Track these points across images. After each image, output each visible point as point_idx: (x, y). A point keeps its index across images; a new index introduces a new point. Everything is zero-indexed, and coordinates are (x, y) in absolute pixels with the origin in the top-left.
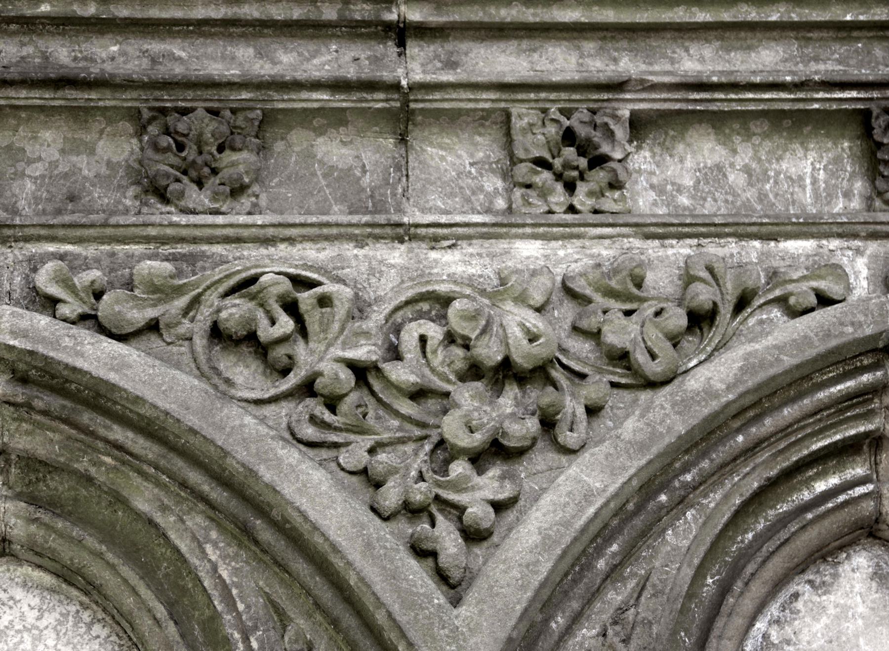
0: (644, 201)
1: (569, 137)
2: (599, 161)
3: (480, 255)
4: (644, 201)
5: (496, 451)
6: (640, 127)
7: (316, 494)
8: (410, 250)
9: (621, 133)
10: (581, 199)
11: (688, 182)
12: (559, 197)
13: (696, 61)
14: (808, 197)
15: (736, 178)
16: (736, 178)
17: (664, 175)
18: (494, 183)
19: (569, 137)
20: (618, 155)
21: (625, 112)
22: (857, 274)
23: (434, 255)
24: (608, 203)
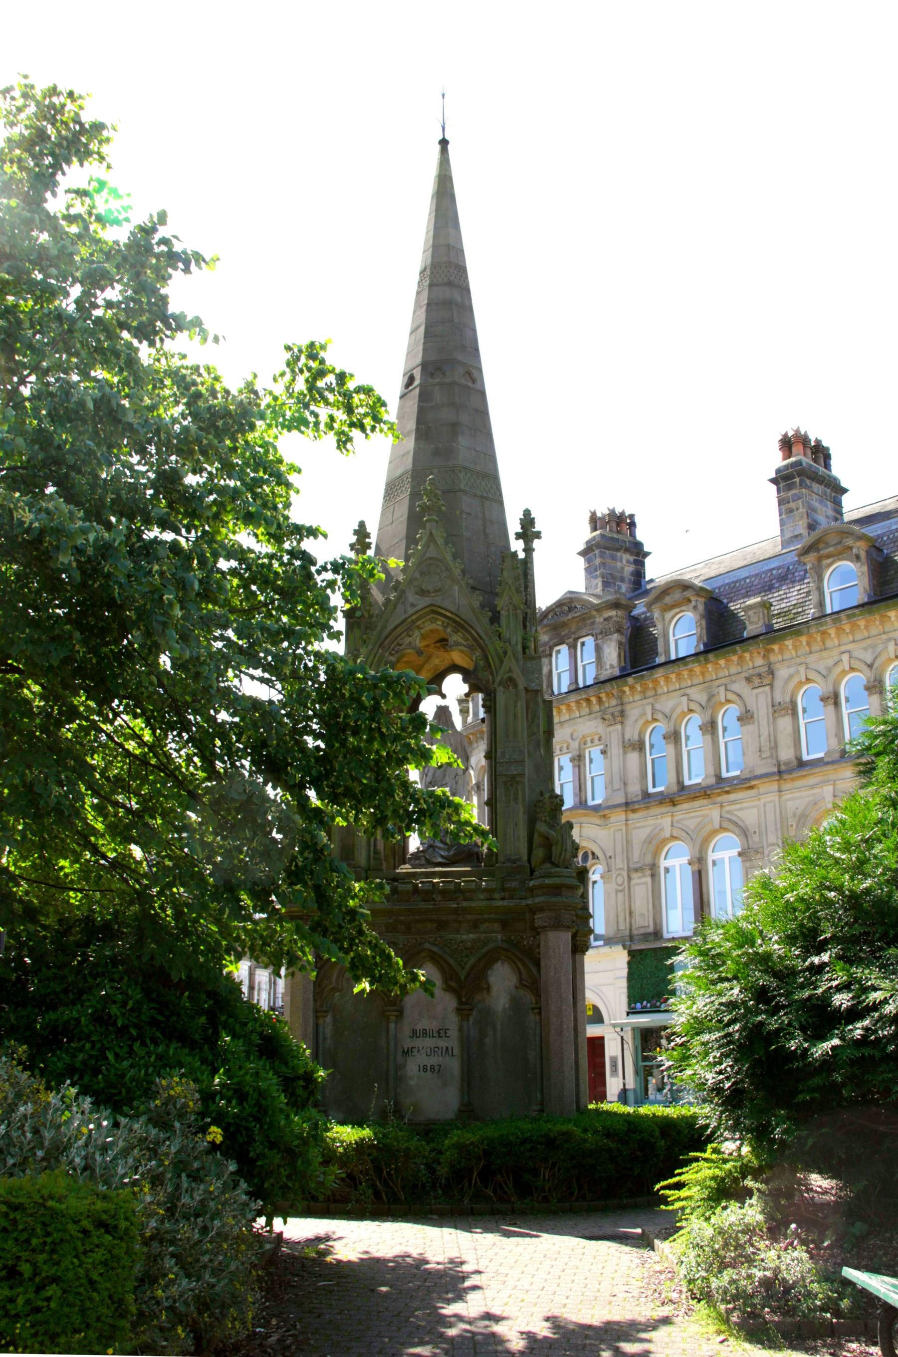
5: (467, 956)
7: (451, 961)
13: (486, 916)
17: (483, 927)
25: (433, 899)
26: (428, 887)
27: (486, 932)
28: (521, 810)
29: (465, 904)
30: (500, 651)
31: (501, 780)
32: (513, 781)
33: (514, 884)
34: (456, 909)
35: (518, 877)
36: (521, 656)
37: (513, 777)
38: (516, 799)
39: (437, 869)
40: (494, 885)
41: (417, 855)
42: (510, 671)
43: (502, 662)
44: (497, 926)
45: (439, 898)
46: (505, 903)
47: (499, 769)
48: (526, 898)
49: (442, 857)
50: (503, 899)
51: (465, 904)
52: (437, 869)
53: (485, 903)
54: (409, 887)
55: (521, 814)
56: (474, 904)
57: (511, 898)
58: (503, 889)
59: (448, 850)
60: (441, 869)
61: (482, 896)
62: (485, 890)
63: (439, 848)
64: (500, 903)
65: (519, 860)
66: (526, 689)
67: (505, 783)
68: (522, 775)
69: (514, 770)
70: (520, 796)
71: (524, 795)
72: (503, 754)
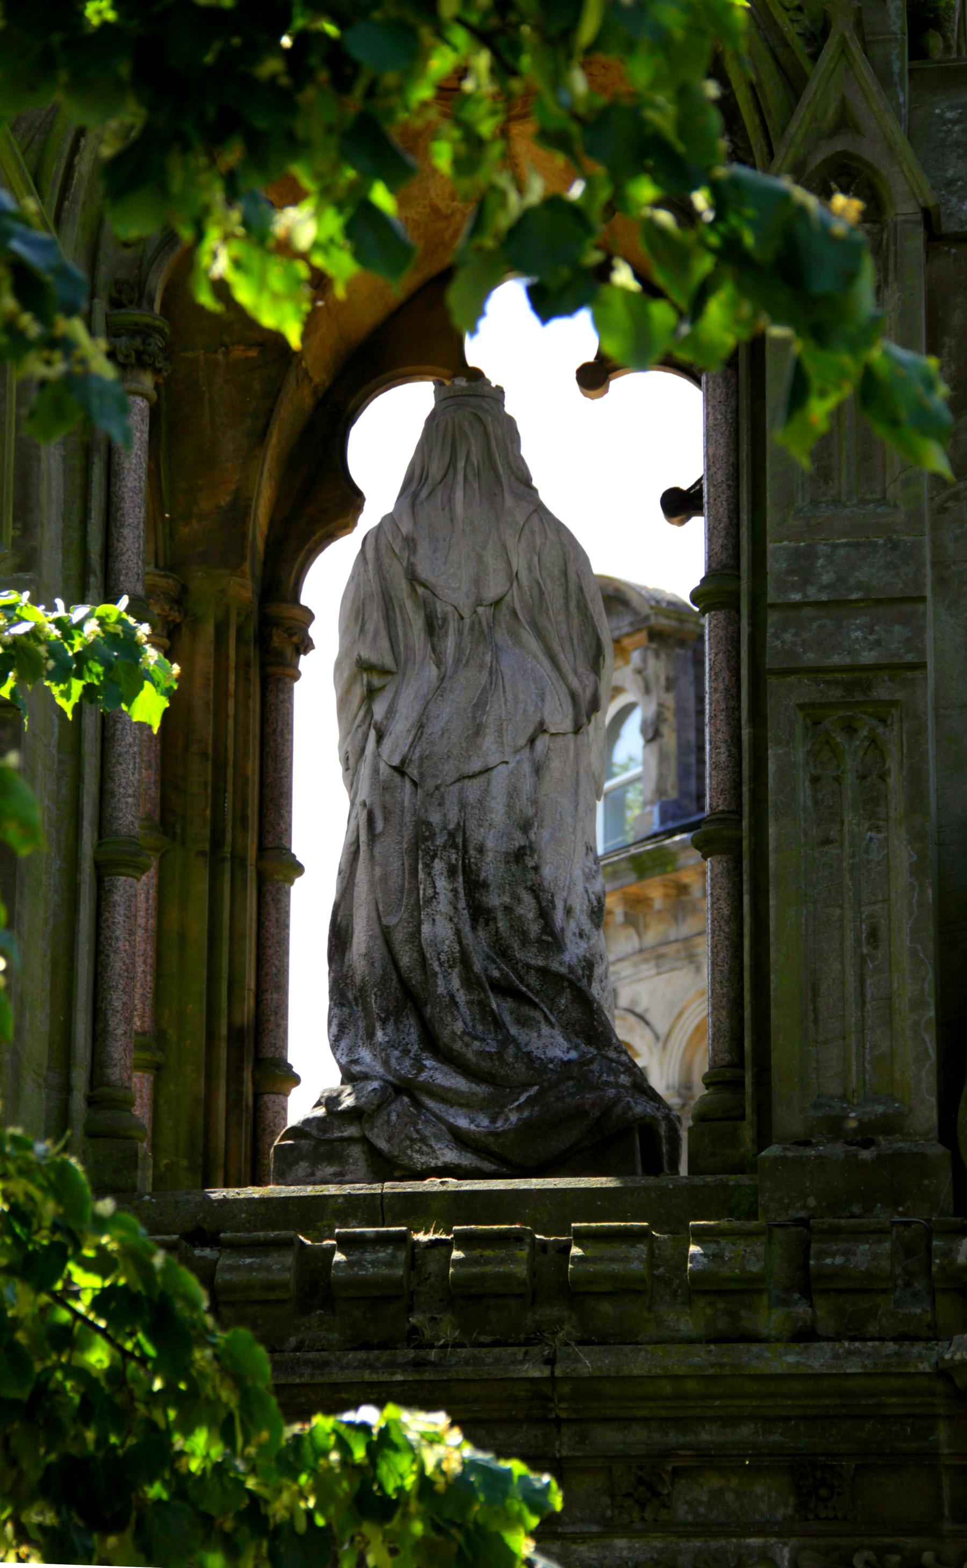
0: (682, 1512)
1: (641, 1481)
2: (657, 1494)
3: (597, 1547)
4: (682, 1512)
6: (676, 1472)
8: (562, 1544)
9: (667, 1478)
10: (648, 1515)
11: (705, 1499)
12: (636, 1514)
13: (707, 1436)
14: (763, 1507)
15: (730, 1497)
16: (730, 1497)
17: (693, 1497)
18: (605, 1500)
19: (641, 1481)
20: (665, 1492)
21: (669, 1468)
22: (782, 1558)
23: (574, 1547)
24: (664, 1515)
25: (413, 1337)
26: (380, 1266)
27: (701, 1528)
28: (903, 855)
29: (588, 1362)
30: (791, 31)
31: (785, 699)
32: (856, 701)
33: (864, 1256)
34: (540, 1394)
35: (882, 1216)
36: (899, 62)
37: (857, 680)
38: (872, 803)
39: (432, 1185)
40: (749, 1257)
41: (323, 1141)
42: (845, 122)
43: (794, 84)
44: (768, 1496)
45: (448, 1331)
46: (818, 1358)
47: (780, 640)
48: (935, 1334)
49: (460, 1139)
50: (805, 1335)
51: (588, 1362)
52: (432, 1185)
53: (701, 1357)
54: (281, 1267)
55: (902, 879)
56: (639, 1362)
57: (853, 1330)
58: (806, 1283)
59: (493, 1107)
60: (452, 1184)
61: (687, 1325)
62: (704, 1287)
63: (445, 1096)
64: (790, 1359)
65: (890, 1125)
66: (929, 218)
67: (813, 714)
68: (907, 670)
69: (860, 643)
70: (894, 781)
71: (916, 777)
72: (802, 564)
